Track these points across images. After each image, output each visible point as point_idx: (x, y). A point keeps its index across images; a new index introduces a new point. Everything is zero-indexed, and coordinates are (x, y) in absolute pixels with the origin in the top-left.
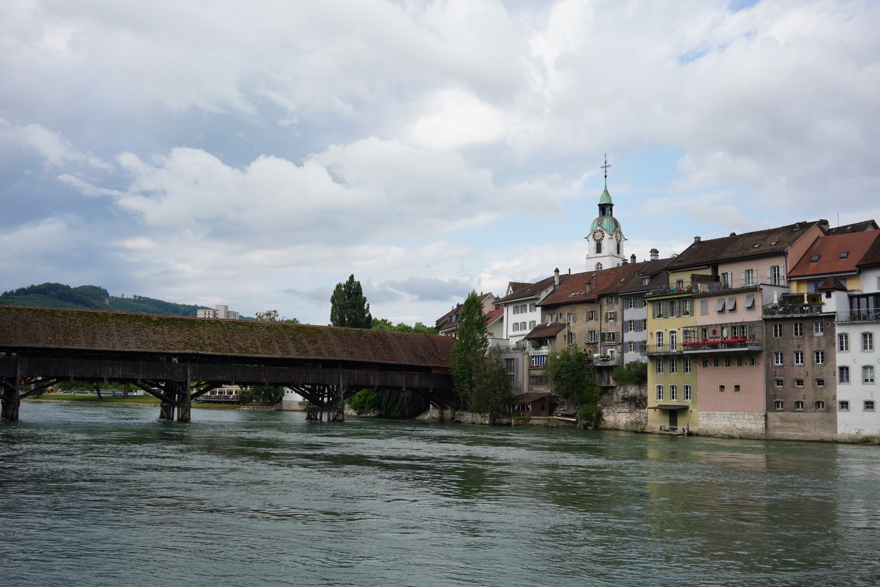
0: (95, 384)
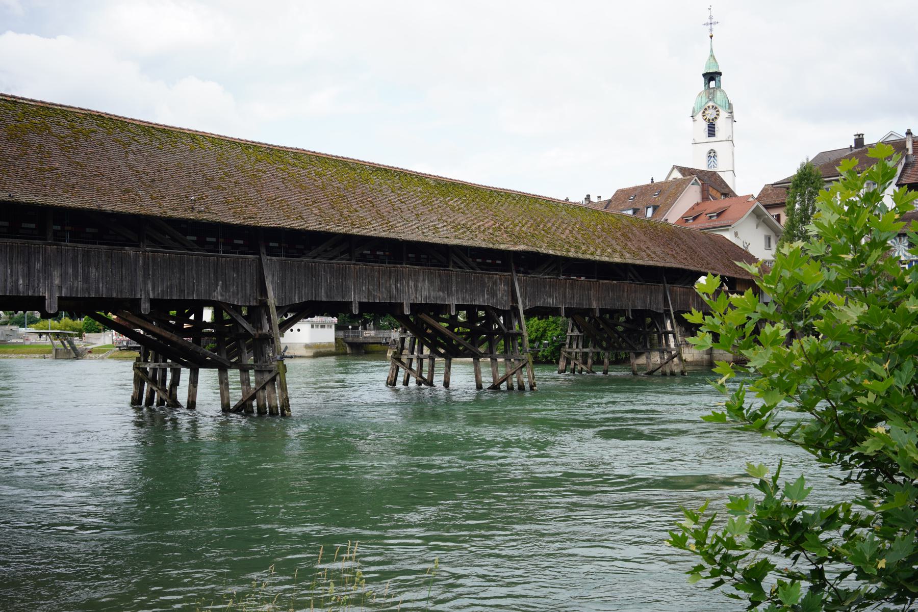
0: (551, 319)
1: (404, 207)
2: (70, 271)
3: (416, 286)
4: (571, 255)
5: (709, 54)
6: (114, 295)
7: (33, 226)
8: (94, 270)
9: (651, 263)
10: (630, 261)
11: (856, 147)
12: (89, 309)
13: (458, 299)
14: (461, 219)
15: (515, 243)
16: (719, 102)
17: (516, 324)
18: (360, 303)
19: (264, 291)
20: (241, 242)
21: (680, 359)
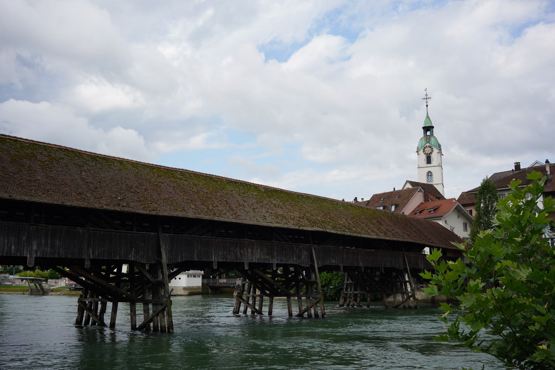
0: (334, 273)
1: (246, 204)
2: (43, 241)
3: (252, 252)
4: (346, 233)
5: (426, 116)
6: (69, 256)
7: (23, 214)
8: (58, 241)
9: (395, 239)
10: (382, 238)
11: (516, 170)
12: (53, 265)
13: (278, 260)
14: (280, 212)
15: (313, 226)
16: (433, 144)
17: (313, 276)
18: (218, 262)
19: (160, 255)
20: (147, 225)
21: (414, 298)
